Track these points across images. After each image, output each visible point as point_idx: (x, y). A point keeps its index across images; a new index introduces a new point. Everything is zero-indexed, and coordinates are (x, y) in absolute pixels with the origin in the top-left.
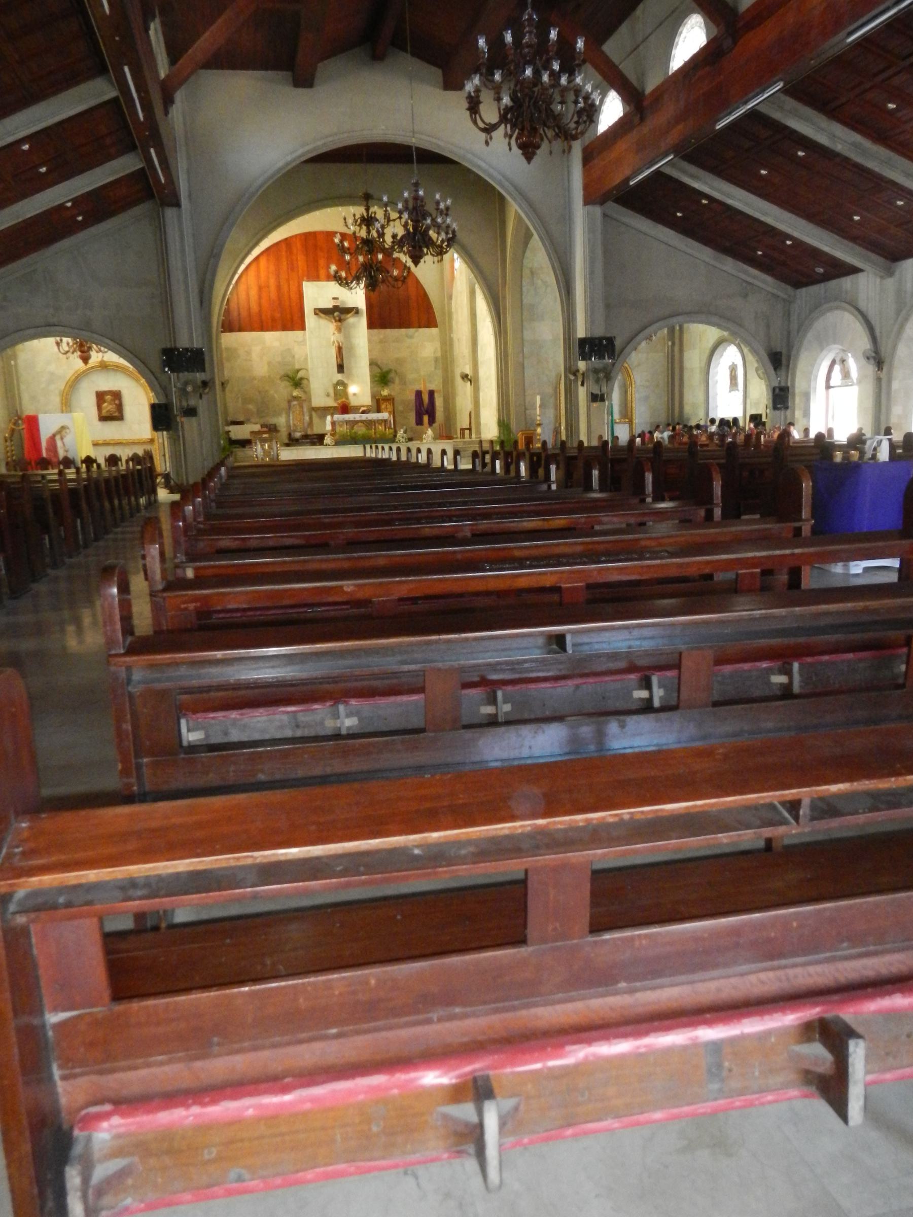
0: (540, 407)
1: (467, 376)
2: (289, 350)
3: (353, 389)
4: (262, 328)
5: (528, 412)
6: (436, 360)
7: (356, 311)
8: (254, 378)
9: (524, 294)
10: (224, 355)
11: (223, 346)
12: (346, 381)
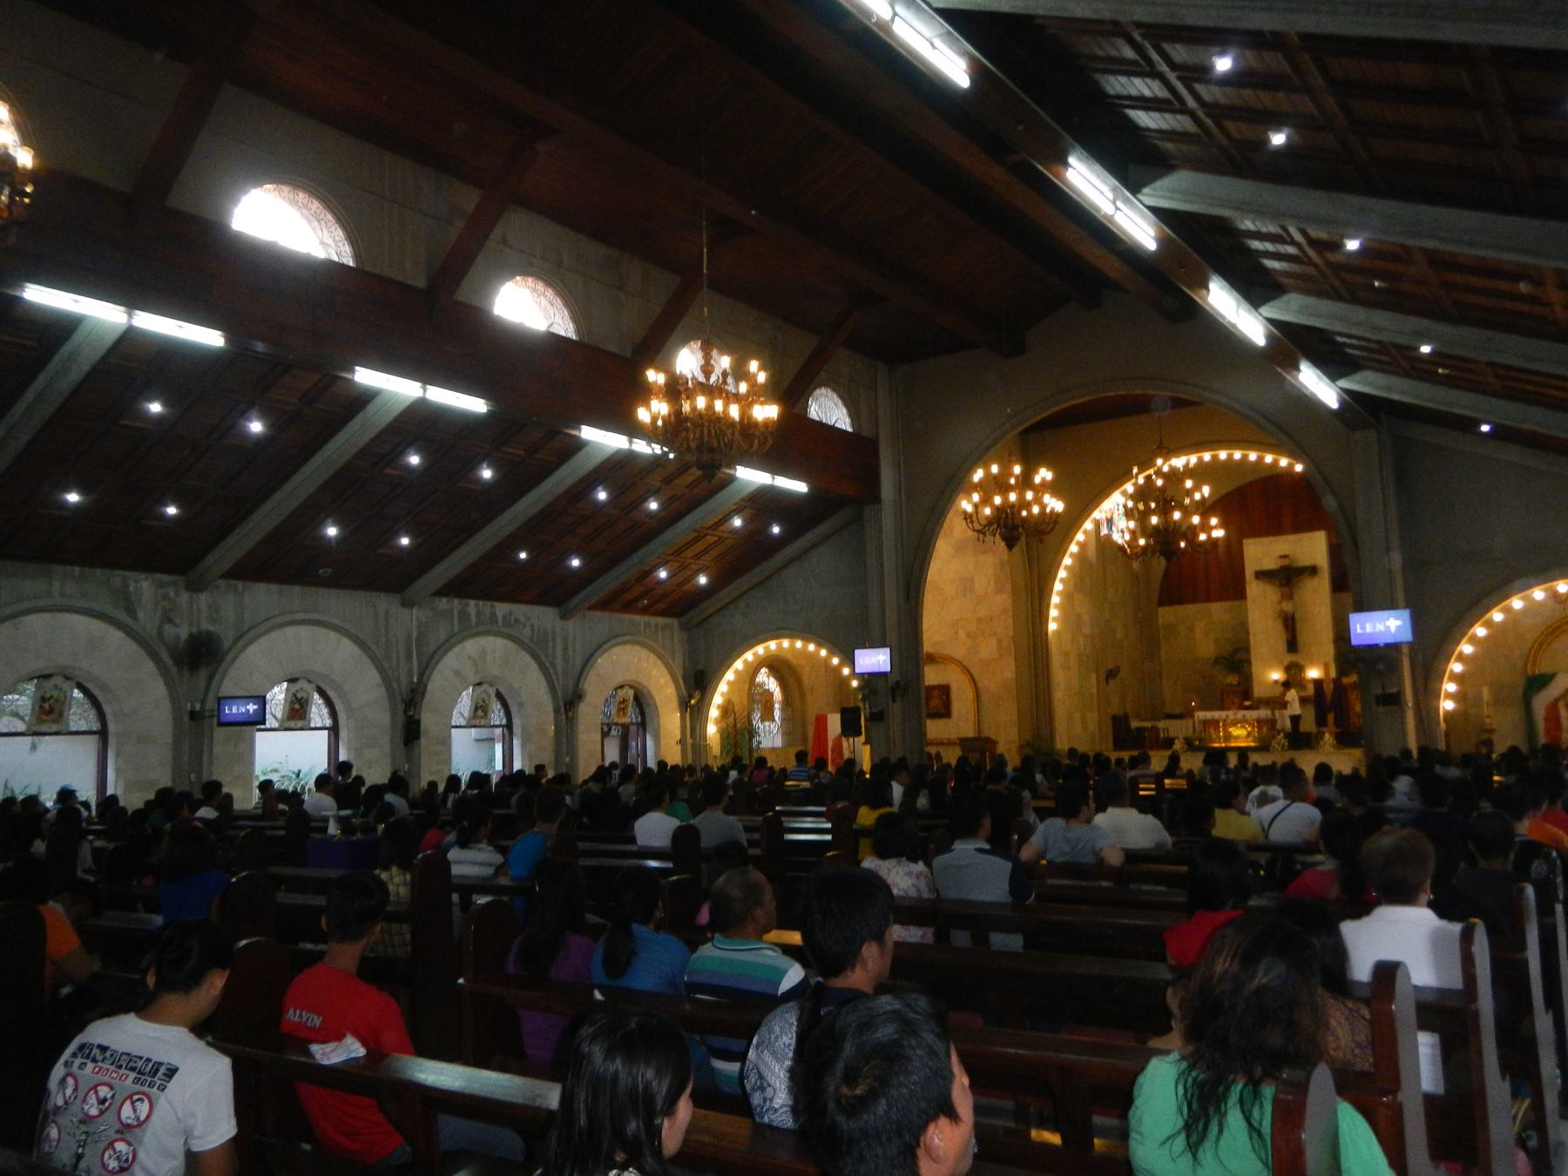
4: (1208, 600)
7: (1313, 570)
10: (1162, 633)
11: (1160, 622)
12: (1302, 663)
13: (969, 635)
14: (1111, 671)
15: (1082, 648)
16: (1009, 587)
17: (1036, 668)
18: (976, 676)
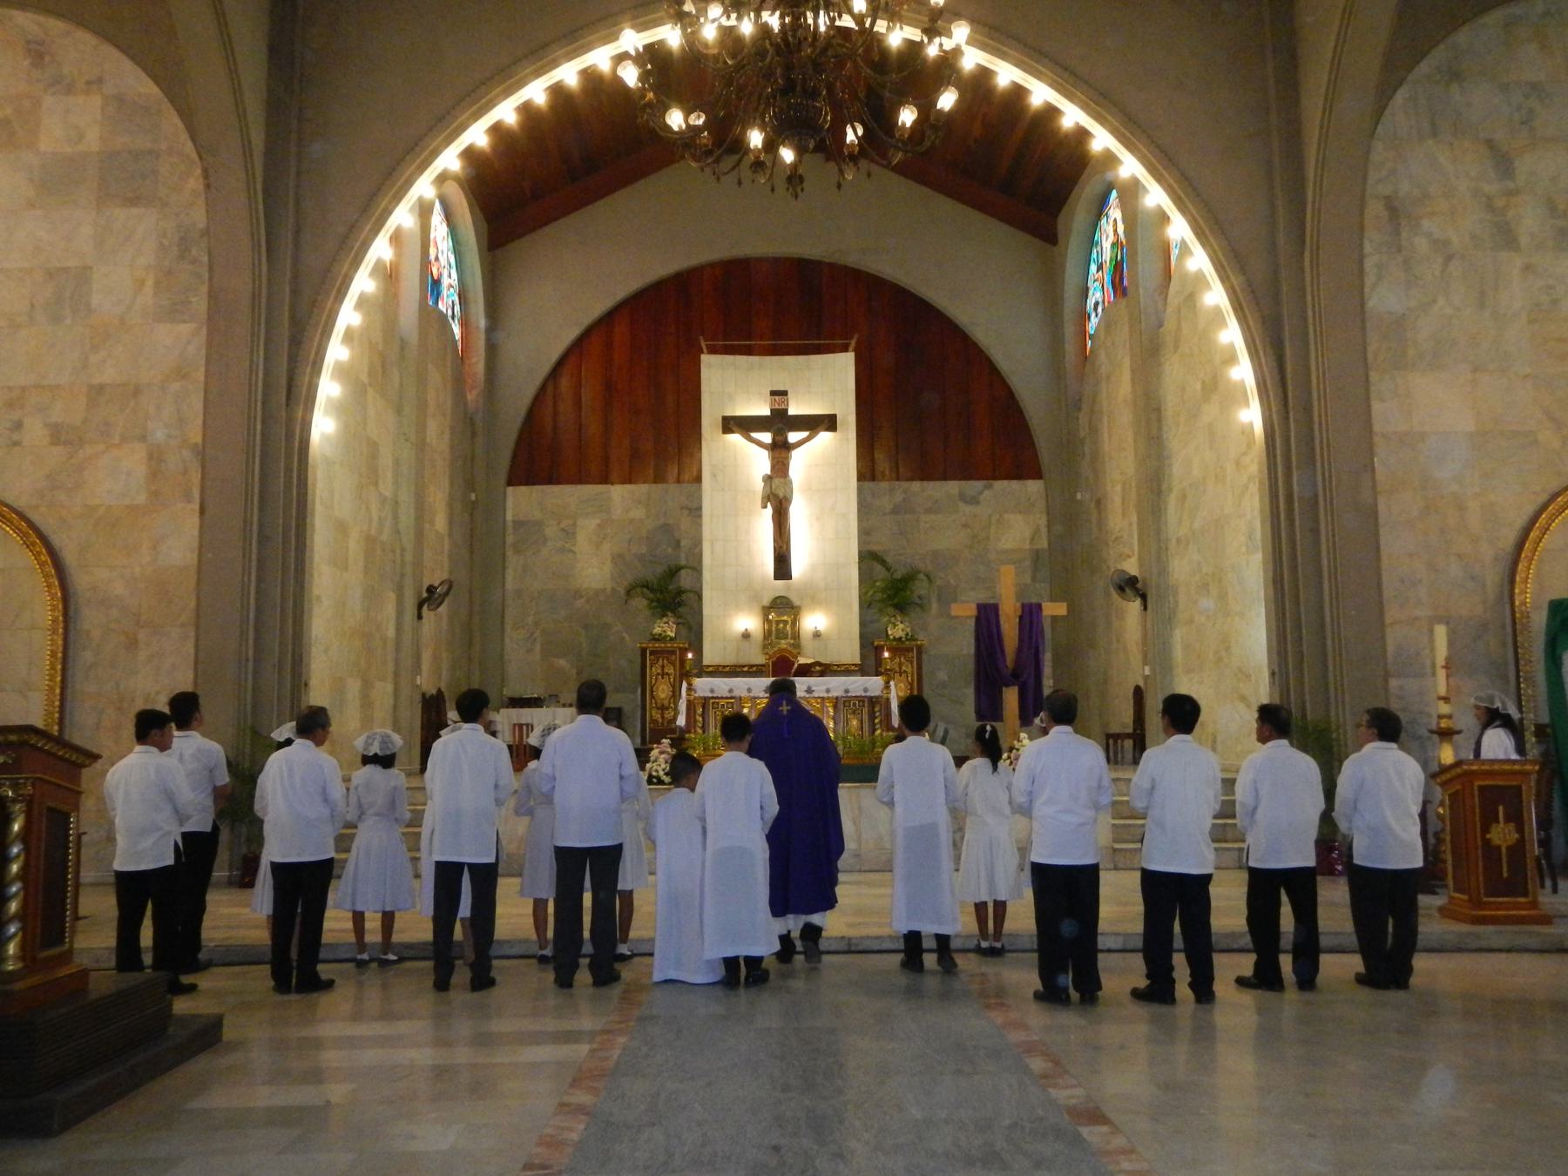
0: (1446, 667)
1: (1132, 581)
2: (667, 529)
3: (814, 621)
4: (605, 479)
5: (1394, 683)
6: (1037, 555)
8: (577, 594)
9: (1369, 280)
10: (510, 539)
11: (509, 517)
13: (57, 435)
14: (431, 590)
15: (375, 524)
16: (200, 303)
17: (263, 539)
18: (70, 557)
